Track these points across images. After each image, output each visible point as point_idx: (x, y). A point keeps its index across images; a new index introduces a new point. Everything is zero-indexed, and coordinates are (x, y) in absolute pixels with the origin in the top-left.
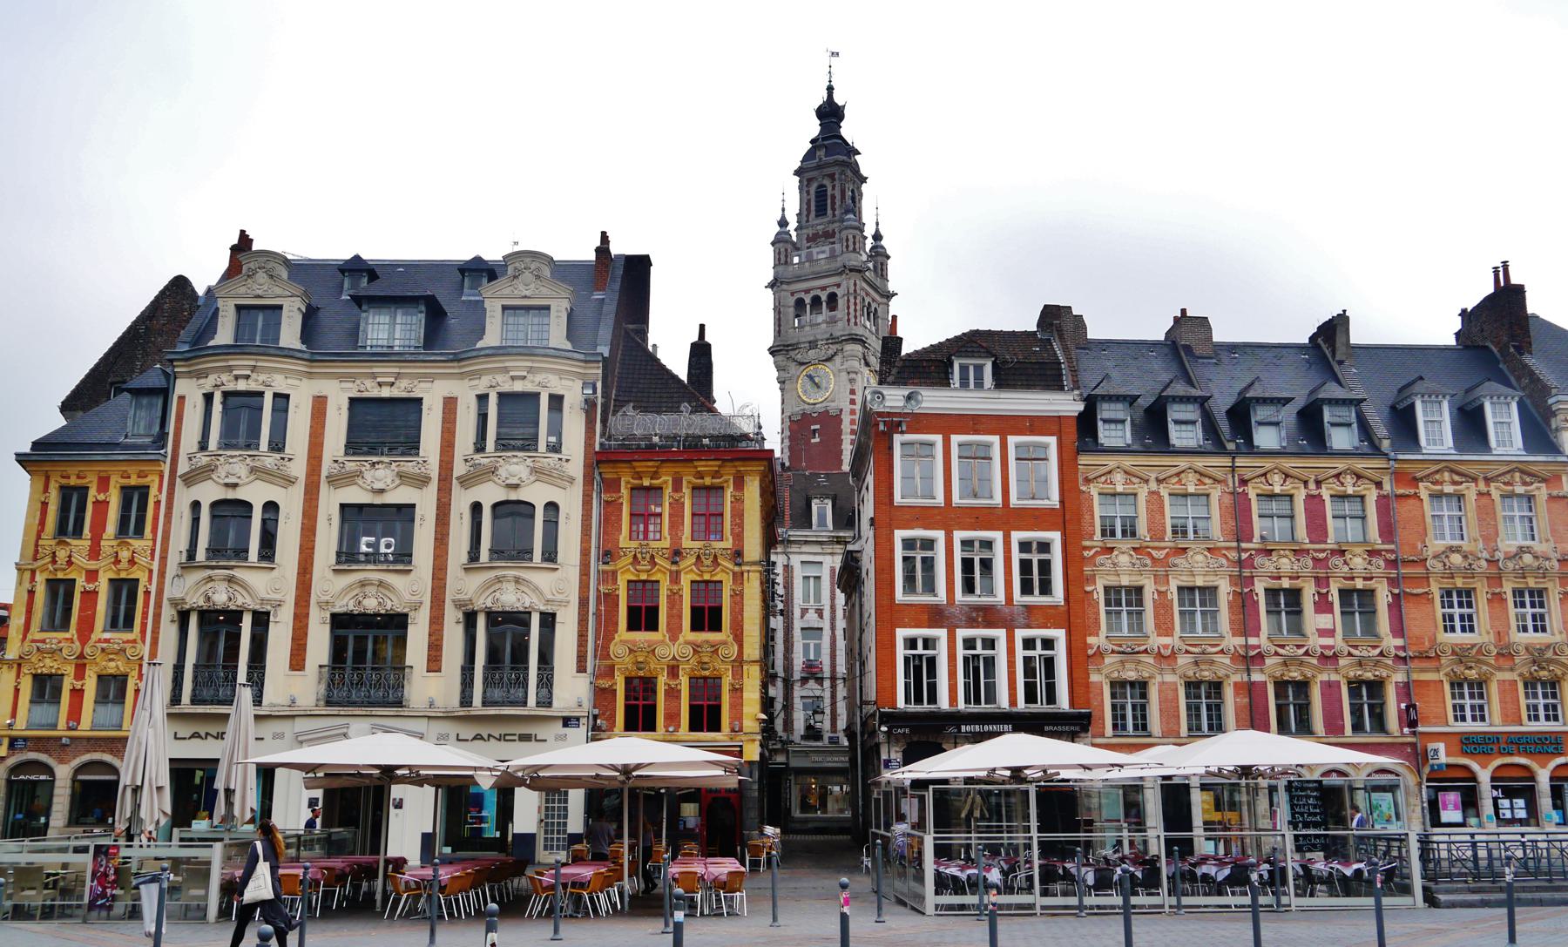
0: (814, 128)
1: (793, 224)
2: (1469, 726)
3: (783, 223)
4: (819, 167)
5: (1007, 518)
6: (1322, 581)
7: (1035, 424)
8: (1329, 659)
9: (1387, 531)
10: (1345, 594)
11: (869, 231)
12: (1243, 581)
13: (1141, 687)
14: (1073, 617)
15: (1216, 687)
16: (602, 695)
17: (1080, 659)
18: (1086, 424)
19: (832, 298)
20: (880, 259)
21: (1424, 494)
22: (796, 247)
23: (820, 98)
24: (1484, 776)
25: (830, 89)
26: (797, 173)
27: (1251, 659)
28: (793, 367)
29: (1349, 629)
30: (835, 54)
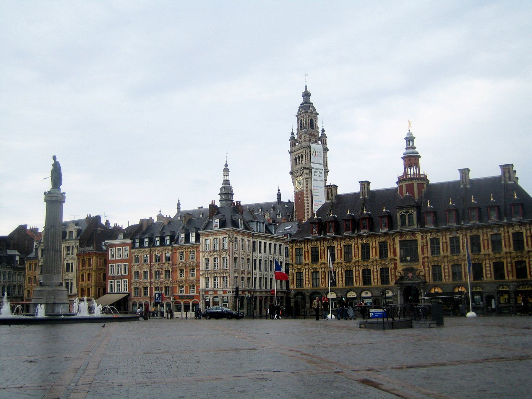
0: (301, 100)
1: (295, 132)
2: (182, 294)
3: (293, 134)
4: (300, 114)
5: (122, 261)
6: (162, 269)
7: (126, 245)
8: (161, 283)
9: (172, 260)
10: (166, 271)
11: (320, 130)
12: (151, 270)
13: (137, 288)
14: (129, 277)
15: (147, 288)
16: (78, 291)
17: (130, 284)
18: (133, 243)
19: (302, 155)
20: (323, 138)
21: (178, 252)
22: (296, 140)
23: (304, 90)
24: (182, 303)
25: (306, 87)
26: (296, 116)
27: (151, 283)
28: (295, 179)
29: (166, 277)
30: (306, 75)
